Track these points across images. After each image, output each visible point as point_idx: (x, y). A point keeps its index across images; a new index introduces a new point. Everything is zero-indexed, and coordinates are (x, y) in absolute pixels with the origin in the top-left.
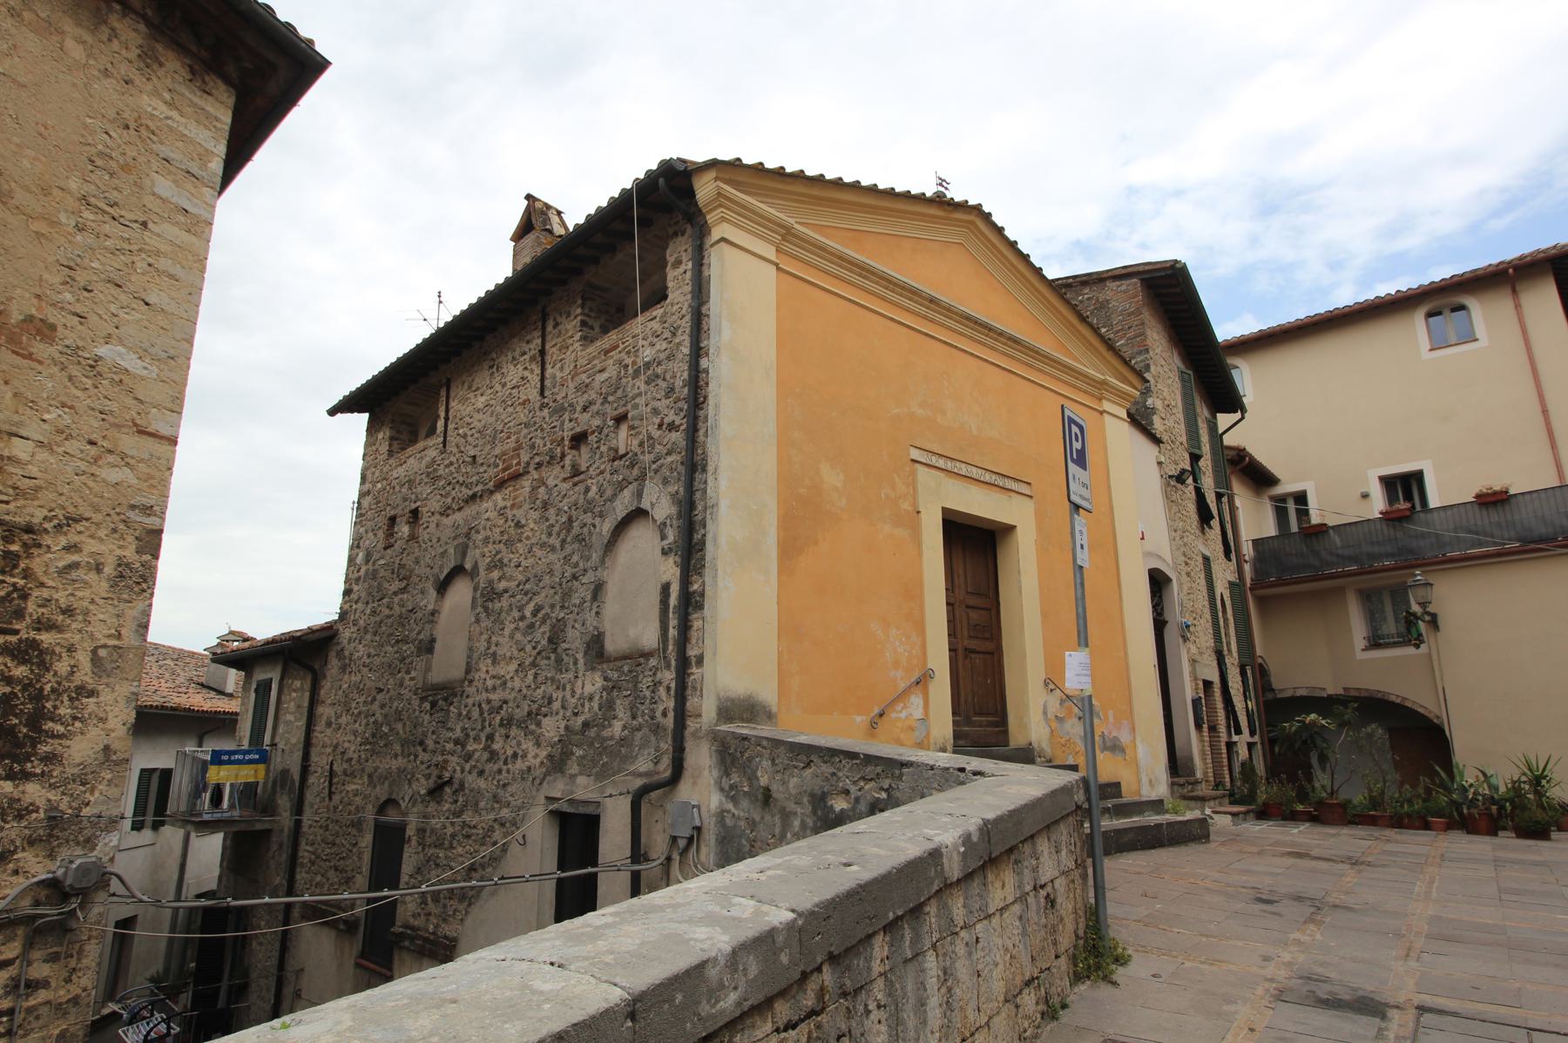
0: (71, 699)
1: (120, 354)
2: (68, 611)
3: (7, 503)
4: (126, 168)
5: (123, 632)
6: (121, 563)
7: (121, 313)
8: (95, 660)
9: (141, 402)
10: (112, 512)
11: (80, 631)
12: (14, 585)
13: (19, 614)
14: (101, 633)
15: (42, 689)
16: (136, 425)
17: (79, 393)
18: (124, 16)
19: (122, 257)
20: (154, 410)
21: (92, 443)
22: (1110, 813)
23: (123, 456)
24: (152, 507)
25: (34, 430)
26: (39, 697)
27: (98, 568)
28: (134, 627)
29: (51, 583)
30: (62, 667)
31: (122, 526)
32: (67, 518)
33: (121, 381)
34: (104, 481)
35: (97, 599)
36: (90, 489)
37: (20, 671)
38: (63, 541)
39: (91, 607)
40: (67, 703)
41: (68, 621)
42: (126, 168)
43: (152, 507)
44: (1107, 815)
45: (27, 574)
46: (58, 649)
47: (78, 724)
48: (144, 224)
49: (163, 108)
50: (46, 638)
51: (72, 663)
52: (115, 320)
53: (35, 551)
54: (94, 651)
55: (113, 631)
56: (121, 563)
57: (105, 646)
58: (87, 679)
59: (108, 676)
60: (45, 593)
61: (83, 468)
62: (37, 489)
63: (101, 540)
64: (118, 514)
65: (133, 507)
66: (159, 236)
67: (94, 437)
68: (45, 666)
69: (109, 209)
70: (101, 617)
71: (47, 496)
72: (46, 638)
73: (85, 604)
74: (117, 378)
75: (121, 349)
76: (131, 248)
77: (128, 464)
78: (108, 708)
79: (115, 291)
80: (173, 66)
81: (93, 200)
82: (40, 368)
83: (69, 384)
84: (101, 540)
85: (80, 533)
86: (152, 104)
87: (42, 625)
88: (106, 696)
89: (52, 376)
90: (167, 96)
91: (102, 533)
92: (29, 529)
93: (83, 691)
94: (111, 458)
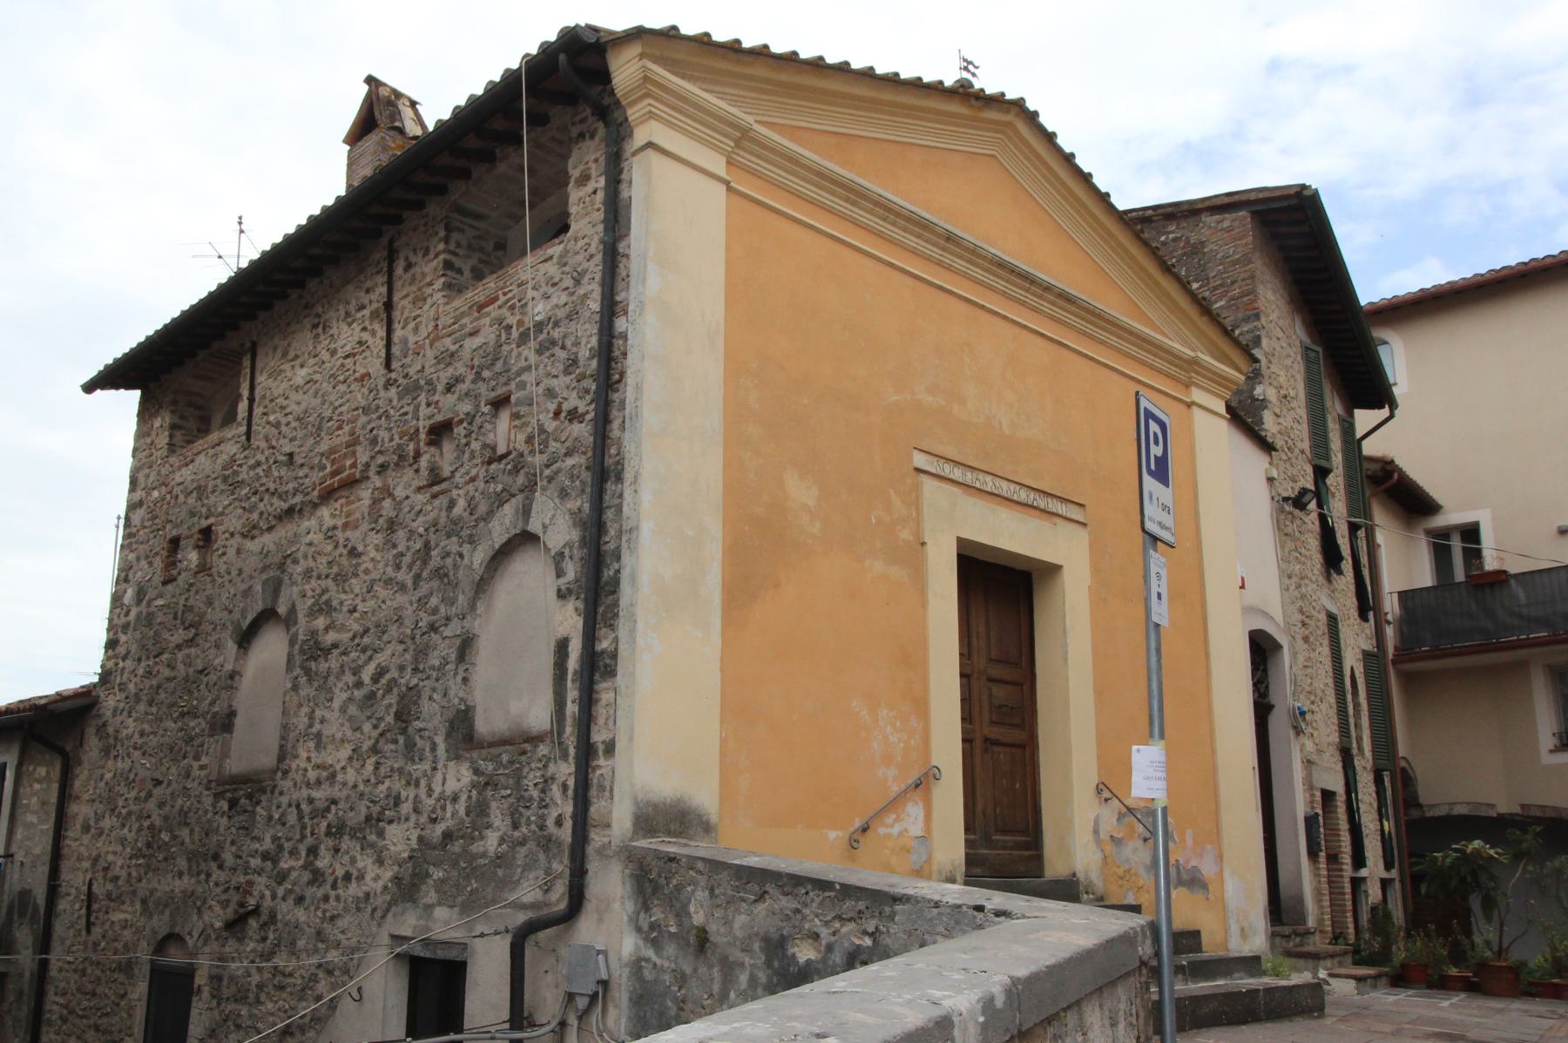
22: (1184, 974)
44: (1180, 976)
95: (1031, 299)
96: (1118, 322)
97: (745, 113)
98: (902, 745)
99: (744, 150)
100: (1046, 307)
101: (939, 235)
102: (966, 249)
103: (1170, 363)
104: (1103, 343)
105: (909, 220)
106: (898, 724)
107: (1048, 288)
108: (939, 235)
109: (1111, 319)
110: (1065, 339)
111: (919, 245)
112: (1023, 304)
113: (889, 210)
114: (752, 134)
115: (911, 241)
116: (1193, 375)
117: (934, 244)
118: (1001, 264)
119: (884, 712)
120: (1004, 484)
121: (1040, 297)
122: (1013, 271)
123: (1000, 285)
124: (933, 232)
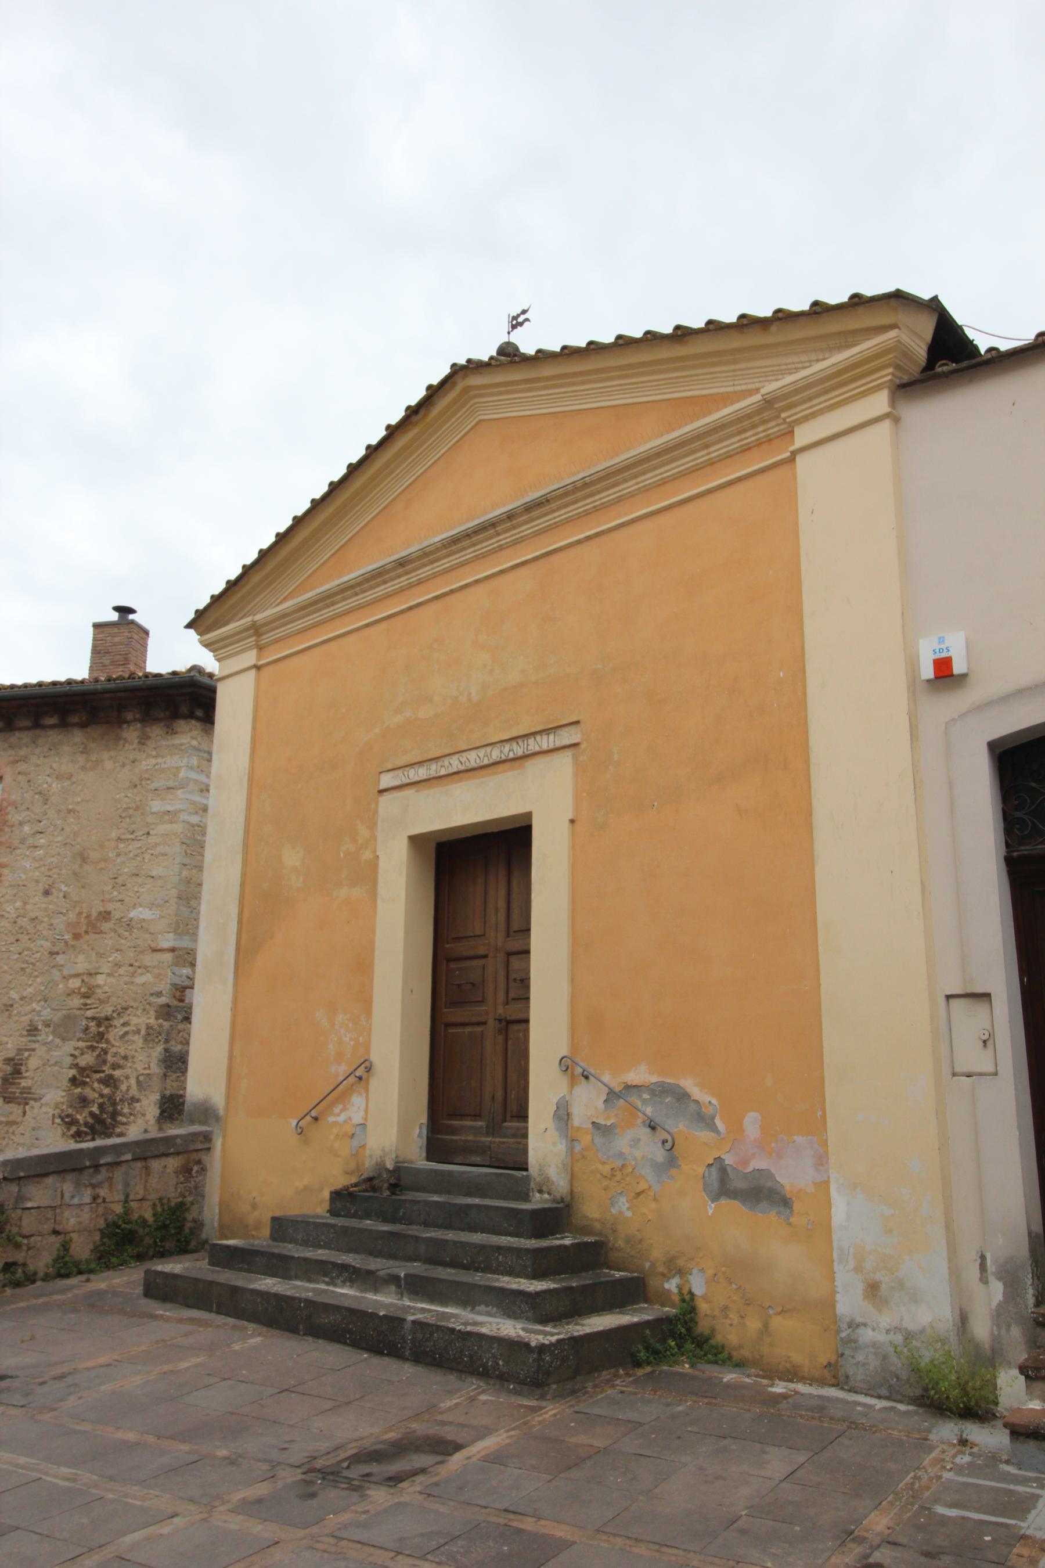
0: (129, 1104)
1: (141, 913)
2: (125, 1058)
3: (97, 1008)
4: (137, 809)
5: (152, 1065)
6: (149, 1027)
7: (141, 890)
8: (139, 1082)
9: (153, 934)
10: (143, 1000)
11: (131, 1067)
12: (102, 1048)
13: (105, 1062)
14: (140, 1067)
15: (115, 1100)
16: (151, 948)
17: (123, 941)
18: (129, 726)
19: (139, 859)
20: (160, 936)
21: (131, 965)
23: (146, 968)
24: (161, 992)
25: (105, 969)
26: (114, 1104)
27: (138, 1032)
28: (156, 1062)
29: (117, 1044)
30: (124, 1088)
31: (147, 1007)
32: (123, 1009)
33: (142, 927)
34: (137, 984)
35: (139, 1050)
36: (131, 990)
37: (106, 1091)
38: (122, 1021)
39: (136, 1054)
40: (127, 1106)
41: (126, 1063)
42: (137, 809)
43: (161, 992)
45: (108, 1042)
46: (122, 1078)
47: (132, 1117)
48: (148, 833)
49: (153, 761)
50: (117, 1073)
51: (128, 1085)
52: (138, 894)
53: (110, 1029)
54: (137, 1078)
55: (146, 1066)
56: (149, 1027)
57: (142, 1074)
58: (135, 1093)
59: (145, 1091)
60: (114, 1050)
61: (128, 980)
62: (109, 997)
63: (139, 1017)
64: (146, 1000)
65: (152, 994)
66: (156, 835)
67: (132, 962)
68: (116, 1087)
69: (131, 837)
70: (140, 1058)
71: (114, 999)
72: (117, 1073)
73: (133, 1053)
74: (139, 926)
75: (140, 909)
76: (142, 851)
77: (148, 971)
78: (146, 1108)
79: (135, 879)
80: (156, 731)
81: (123, 837)
82: (105, 936)
83: (118, 939)
84: (139, 1017)
85: (129, 1015)
86: (146, 764)
87: (115, 1066)
88: (145, 1102)
89: (111, 938)
90: (154, 753)
91: (139, 1013)
92: (107, 1019)
93: (134, 1100)
94: (139, 971)
95: (505, 538)
98: (352, 1043)
99: (265, 633)
101: (394, 569)
102: (419, 558)
103: (739, 433)
104: (620, 500)
106: (350, 1025)
108: (394, 569)
112: (501, 548)
113: (352, 587)
114: (258, 624)
115: (381, 590)
117: (399, 576)
118: (455, 540)
119: (340, 1018)
122: (468, 535)
123: (469, 554)
124: (387, 572)
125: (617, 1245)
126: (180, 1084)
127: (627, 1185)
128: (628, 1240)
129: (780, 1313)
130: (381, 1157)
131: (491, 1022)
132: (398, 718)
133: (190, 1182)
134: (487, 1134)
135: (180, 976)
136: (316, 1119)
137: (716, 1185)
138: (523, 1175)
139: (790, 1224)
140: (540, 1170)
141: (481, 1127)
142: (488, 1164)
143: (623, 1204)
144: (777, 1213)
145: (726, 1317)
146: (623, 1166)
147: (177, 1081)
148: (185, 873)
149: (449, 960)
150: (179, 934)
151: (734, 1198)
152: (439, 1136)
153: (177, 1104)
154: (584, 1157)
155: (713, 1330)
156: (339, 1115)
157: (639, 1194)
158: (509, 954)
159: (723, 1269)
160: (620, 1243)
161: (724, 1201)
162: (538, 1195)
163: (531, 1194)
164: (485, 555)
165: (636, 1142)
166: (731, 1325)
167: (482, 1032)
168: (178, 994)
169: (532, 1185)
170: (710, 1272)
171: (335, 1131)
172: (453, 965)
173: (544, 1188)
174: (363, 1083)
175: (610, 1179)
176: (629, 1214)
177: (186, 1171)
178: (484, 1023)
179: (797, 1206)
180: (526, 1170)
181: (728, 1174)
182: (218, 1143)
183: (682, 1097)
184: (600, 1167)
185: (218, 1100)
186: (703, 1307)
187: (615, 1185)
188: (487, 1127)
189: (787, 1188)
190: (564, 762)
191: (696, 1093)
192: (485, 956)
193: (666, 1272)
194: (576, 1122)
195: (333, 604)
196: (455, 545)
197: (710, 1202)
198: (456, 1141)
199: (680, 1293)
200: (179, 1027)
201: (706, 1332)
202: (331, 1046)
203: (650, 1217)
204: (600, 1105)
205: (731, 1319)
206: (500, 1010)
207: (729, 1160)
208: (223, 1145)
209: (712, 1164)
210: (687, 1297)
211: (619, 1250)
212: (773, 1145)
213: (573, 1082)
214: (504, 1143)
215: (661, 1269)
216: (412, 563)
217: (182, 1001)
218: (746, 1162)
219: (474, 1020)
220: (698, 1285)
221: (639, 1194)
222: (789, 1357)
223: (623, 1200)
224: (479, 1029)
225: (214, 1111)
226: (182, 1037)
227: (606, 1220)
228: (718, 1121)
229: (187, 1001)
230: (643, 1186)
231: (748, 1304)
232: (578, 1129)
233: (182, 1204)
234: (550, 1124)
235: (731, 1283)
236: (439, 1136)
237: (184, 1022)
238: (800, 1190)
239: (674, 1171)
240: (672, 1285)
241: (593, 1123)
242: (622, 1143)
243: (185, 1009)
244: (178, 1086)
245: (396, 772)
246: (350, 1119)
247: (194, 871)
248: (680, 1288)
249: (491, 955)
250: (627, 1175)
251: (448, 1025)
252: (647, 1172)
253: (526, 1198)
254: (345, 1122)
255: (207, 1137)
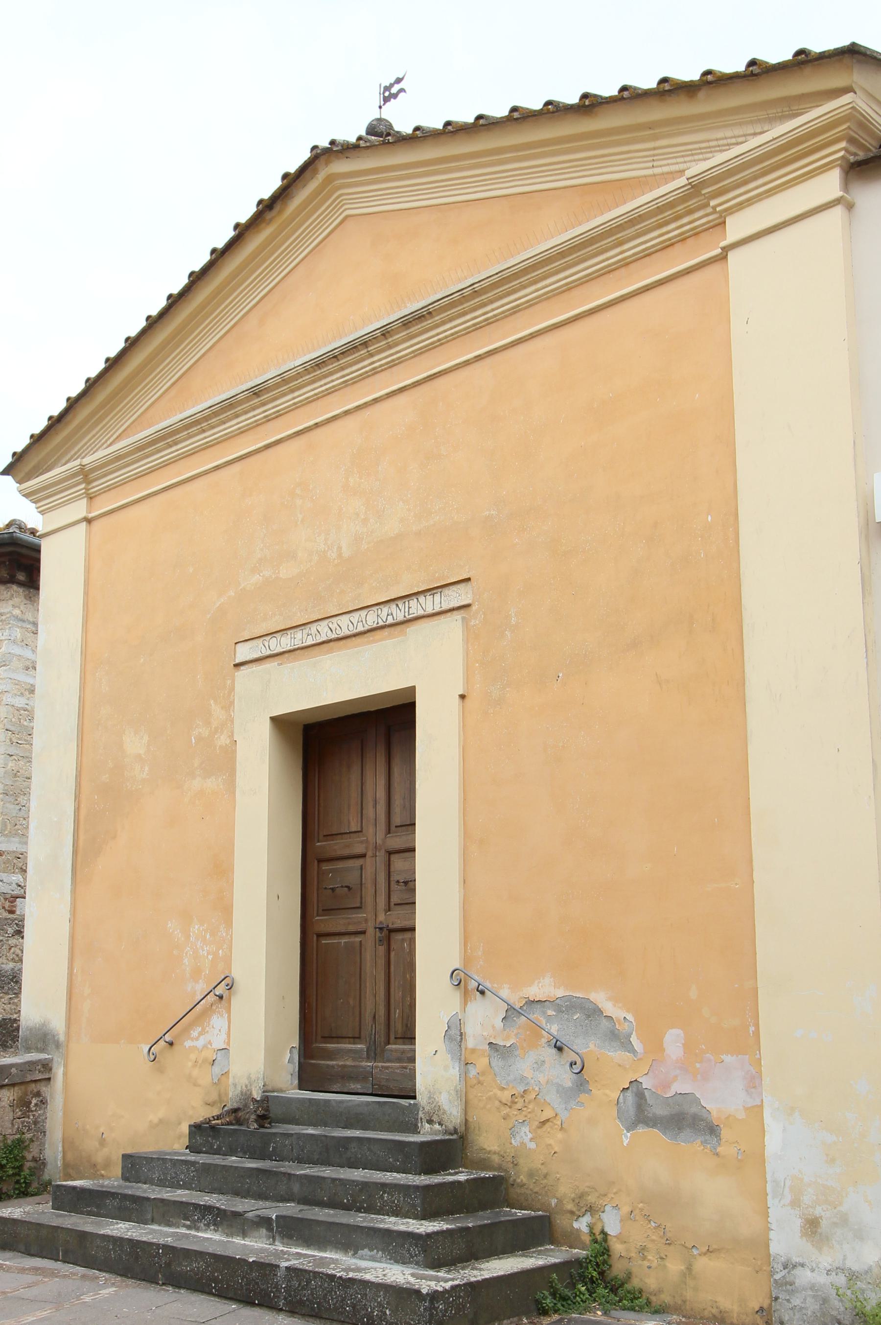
96: (506, 274)
97: (65, 464)
98: (210, 957)
100: (404, 349)
101: (247, 399)
102: (277, 386)
105: (216, 414)
107: (385, 333)
108: (247, 399)
109: (495, 279)
110: (433, 368)
111: (243, 421)
112: (375, 372)
113: (197, 422)
114: (87, 468)
115: (233, 425)
116: (713, 203)
117: (254, 409)
118: (319, 363)
119: (196, 928)
120: (344, 620)
121: (390, 347)
123: (336, 379)
124: (240, 403)
125: (519, 1181)
126: (13, 1007)
127: (529, 1112)
128: (531, 1174)
129: (705, 1254)
130: (246, 1086)
131: (371, 931)
132: (256, 578)
133: (29, 1118)
134: (368, 1058)
135: (10, 884)
136: (171, 1044)
137: (632, 1111)
138: (410, 1104)
139: (717, 1154)
140: (430, 1098)
141: (361, 1050)
142: (370, 1092)
143: (525, 1136)
144: (702, 1142)
145: (644, 1258)
146: (525, 1091)
147: (10, 1003)
148: (11, 764)
149: (320, 861)
150: (6, 836)
151: (654, 1126)
152: (313, 1061)
153: (11, 1029)
154: (479, 1082)
155: (629, 1275)
156: (197, 1039)
157: (544, 1123)
158: (390, 853)
159: (641, 1205)
160: (523, 1178)
161: (641, 1130)
162: (427, 1126)
163: (419, 1125)
164: (355, 381)
165: (539, 1065)
166: (649, 1267)
167: (361, 941)
168: (7, 904)
169: (421, 1115)
170: (626, 1209)
171: (193, 1057)
172: (325, 867)
173: (435, 1118)
174: (223, 1002)
175: (510, 1107)
176: (532, 1145)
177: (24, 1104)
178: (363, 932)
179: (725, 1133)
180: (414, 1098)
181: (646, 1100)
182: (59, 1072)
183: (593, 1012)
184: (499, 1093)
185: (58, 1024)
186: (617, 1248)
187: (515, 1113)
188: (368, 1049)
189: (714, 1114)
190: (453, 625)
191: (609, 1008)
192: (363, 856)
193: (574, 1209)
194: (470, 1043)
195: (176, 443)
196: (320, 369)
197: (625, 1131)
198: (333, 1066)
199: (592, 1233)
200: (10, 942)
201: (621, 1276)
202: (186, 961)
203: (556, 1149)
204: (499, 1024)
205: (649, 1260)
206: (381, 917)
207: (647, 1083)
208: (65, 1074)
209: (628, 1088)
210: (599, 1238)
211: (522, 1185)
212: (698, 1065)
213: (466, 997)
214: (387, 1068)
215: (570, 1206)
216: (268, 393)
217: (12, 912)
218: (667, 1086)
219: (352, 928)
220: (612, 1224)
221: (544, 1123)
222: (716, 1302)
223: (525, 1129)
224: (357, 939)
225: (54, 1036)
226: (14, 953)
227: (505, 1152)
228: (634, 1039)
229: (18, 912)
230: (548, 1114)
231: (669, 1244)
232: (473, 1051)
233: (20, 1142)
234: (441, 1046)
235: (650, 1221)
236: (313, 1061)
237: (16, 937)
238: (730, 1116)
239: (583, 1097)
240: (582, 1225)
241: (490, 1043)
242: (524, 1066)
243: (17, 922)
244: (11, 1009)
245: (255, 642)
246: (210, 1043)
247: (22, 763)
248: (591, 1227)
249: (370, 854)
250: (529, 1102)
251: (320, 935)
252: (552, 1098)
253: (415, 1130)
254: (205, 1047)
255: (46, 1066)
